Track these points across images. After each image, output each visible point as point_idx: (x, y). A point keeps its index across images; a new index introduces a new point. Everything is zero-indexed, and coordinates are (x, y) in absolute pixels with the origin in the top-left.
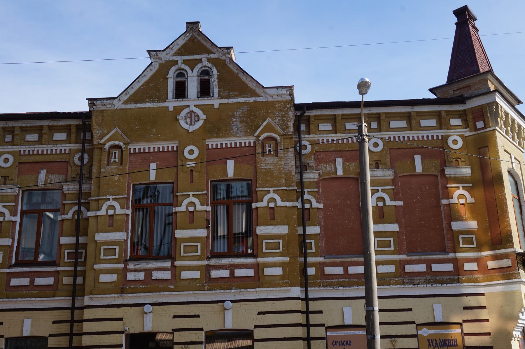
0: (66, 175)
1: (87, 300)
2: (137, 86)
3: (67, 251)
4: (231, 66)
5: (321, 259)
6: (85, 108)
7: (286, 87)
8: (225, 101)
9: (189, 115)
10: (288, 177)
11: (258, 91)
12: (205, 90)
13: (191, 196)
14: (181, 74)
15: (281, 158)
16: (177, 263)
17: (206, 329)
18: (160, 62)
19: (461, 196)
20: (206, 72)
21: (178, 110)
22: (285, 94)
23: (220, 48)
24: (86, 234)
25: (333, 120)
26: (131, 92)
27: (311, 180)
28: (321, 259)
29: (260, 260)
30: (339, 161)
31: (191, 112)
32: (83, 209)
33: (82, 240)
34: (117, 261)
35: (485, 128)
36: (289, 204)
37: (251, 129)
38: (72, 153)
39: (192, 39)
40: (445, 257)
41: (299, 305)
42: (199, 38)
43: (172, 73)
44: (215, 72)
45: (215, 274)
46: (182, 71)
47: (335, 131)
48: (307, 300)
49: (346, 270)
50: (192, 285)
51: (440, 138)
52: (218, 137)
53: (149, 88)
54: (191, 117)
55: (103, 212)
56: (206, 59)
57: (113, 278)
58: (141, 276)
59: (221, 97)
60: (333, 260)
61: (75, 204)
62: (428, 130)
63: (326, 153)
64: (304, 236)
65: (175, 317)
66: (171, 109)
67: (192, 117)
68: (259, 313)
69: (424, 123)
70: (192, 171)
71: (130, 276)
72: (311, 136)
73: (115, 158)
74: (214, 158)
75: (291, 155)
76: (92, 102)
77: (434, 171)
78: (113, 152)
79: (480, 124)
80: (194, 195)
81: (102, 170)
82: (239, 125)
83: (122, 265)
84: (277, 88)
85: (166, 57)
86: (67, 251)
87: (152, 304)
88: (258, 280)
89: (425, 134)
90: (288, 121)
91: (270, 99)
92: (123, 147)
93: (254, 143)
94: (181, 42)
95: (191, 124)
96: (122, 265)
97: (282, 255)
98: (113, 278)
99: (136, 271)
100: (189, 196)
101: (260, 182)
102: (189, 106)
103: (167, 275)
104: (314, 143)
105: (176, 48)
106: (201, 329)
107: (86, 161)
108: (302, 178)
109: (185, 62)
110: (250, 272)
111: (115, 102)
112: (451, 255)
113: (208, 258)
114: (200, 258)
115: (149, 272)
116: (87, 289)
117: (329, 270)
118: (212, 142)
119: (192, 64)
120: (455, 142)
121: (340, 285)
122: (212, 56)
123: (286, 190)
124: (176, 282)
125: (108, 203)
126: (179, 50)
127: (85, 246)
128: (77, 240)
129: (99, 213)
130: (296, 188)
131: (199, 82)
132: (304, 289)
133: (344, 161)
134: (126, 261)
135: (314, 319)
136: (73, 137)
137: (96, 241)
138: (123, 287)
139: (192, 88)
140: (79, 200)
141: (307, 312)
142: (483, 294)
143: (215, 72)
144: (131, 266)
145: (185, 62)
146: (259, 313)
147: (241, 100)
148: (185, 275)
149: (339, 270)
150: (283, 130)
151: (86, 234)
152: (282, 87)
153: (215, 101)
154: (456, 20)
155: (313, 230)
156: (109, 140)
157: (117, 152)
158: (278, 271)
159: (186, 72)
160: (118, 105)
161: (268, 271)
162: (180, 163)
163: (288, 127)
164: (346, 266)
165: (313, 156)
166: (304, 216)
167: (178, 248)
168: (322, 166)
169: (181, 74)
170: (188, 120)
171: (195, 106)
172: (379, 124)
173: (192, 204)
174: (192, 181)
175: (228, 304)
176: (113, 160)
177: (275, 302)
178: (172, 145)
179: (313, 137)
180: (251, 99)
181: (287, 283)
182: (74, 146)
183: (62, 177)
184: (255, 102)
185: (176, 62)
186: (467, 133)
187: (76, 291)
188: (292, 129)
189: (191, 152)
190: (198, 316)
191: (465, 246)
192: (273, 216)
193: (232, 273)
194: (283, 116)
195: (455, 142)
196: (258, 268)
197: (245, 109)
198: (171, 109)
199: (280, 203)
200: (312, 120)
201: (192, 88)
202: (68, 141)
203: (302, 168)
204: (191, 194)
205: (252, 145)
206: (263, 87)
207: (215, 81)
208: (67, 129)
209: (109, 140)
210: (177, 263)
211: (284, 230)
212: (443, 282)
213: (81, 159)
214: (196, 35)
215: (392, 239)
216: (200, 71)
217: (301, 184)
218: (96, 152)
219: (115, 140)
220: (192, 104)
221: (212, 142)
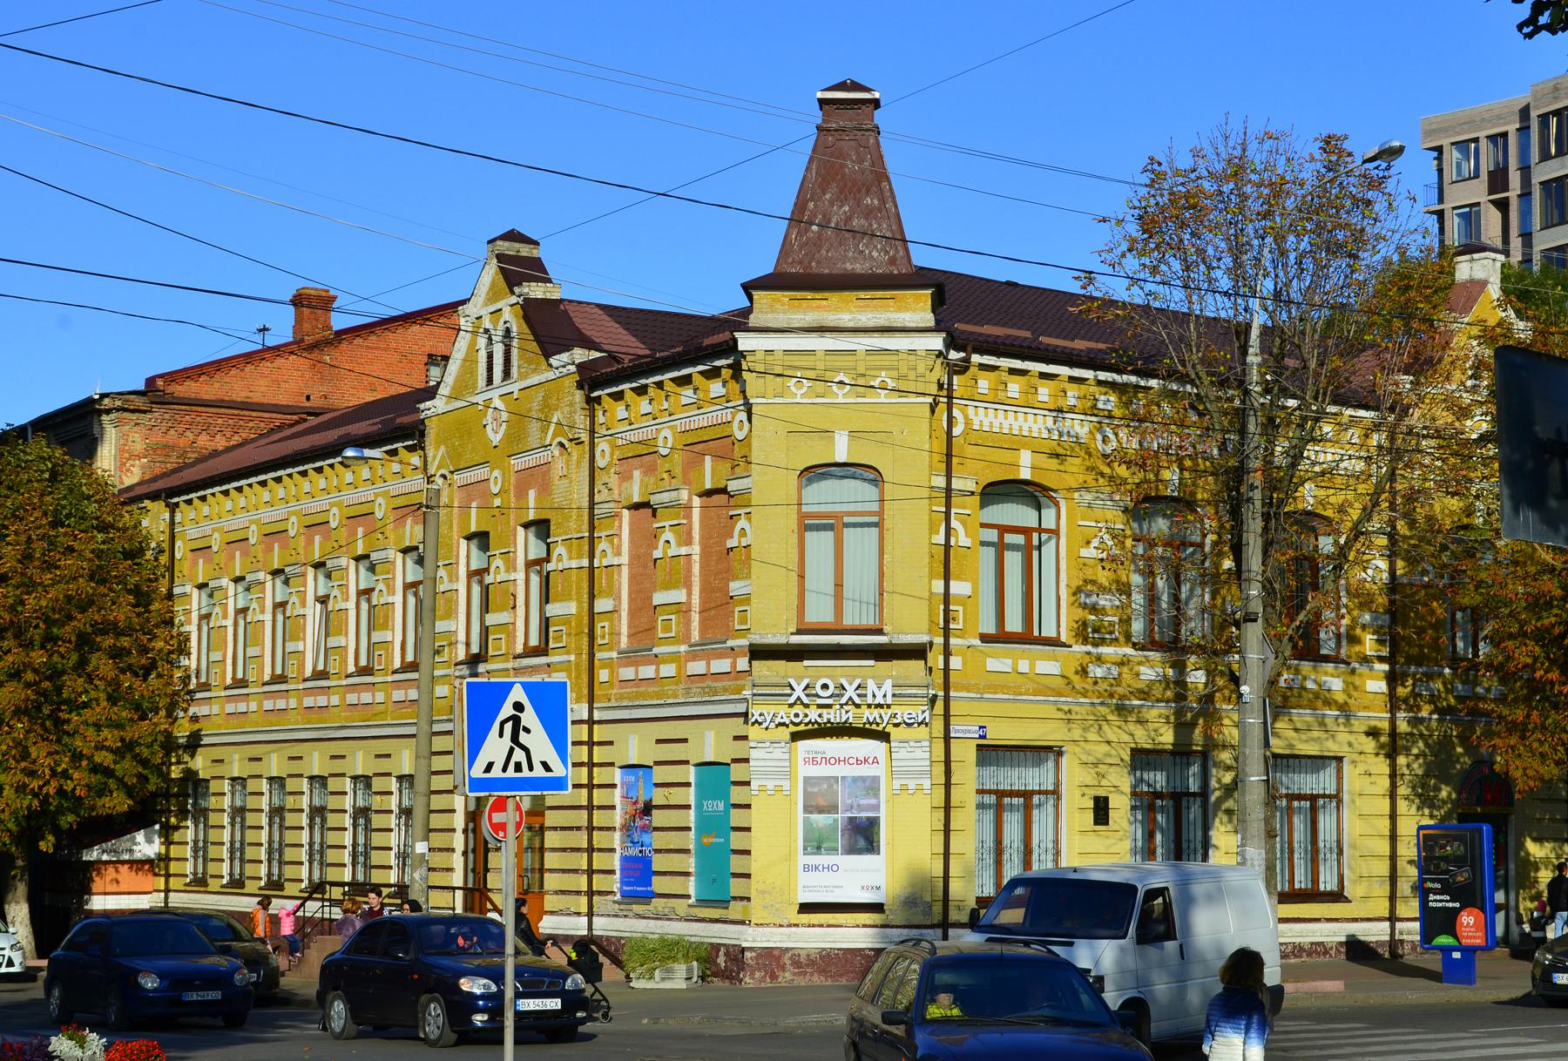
20: (508, 331)
30: (637, 474)
43: (482, 342)
104: (614, 447)
118: (517, 463)
135: (599, 754)
153: (515, 388)
155: (602, 605)
194: (571, 405)
195: (741, 429)
199: (566, 564)
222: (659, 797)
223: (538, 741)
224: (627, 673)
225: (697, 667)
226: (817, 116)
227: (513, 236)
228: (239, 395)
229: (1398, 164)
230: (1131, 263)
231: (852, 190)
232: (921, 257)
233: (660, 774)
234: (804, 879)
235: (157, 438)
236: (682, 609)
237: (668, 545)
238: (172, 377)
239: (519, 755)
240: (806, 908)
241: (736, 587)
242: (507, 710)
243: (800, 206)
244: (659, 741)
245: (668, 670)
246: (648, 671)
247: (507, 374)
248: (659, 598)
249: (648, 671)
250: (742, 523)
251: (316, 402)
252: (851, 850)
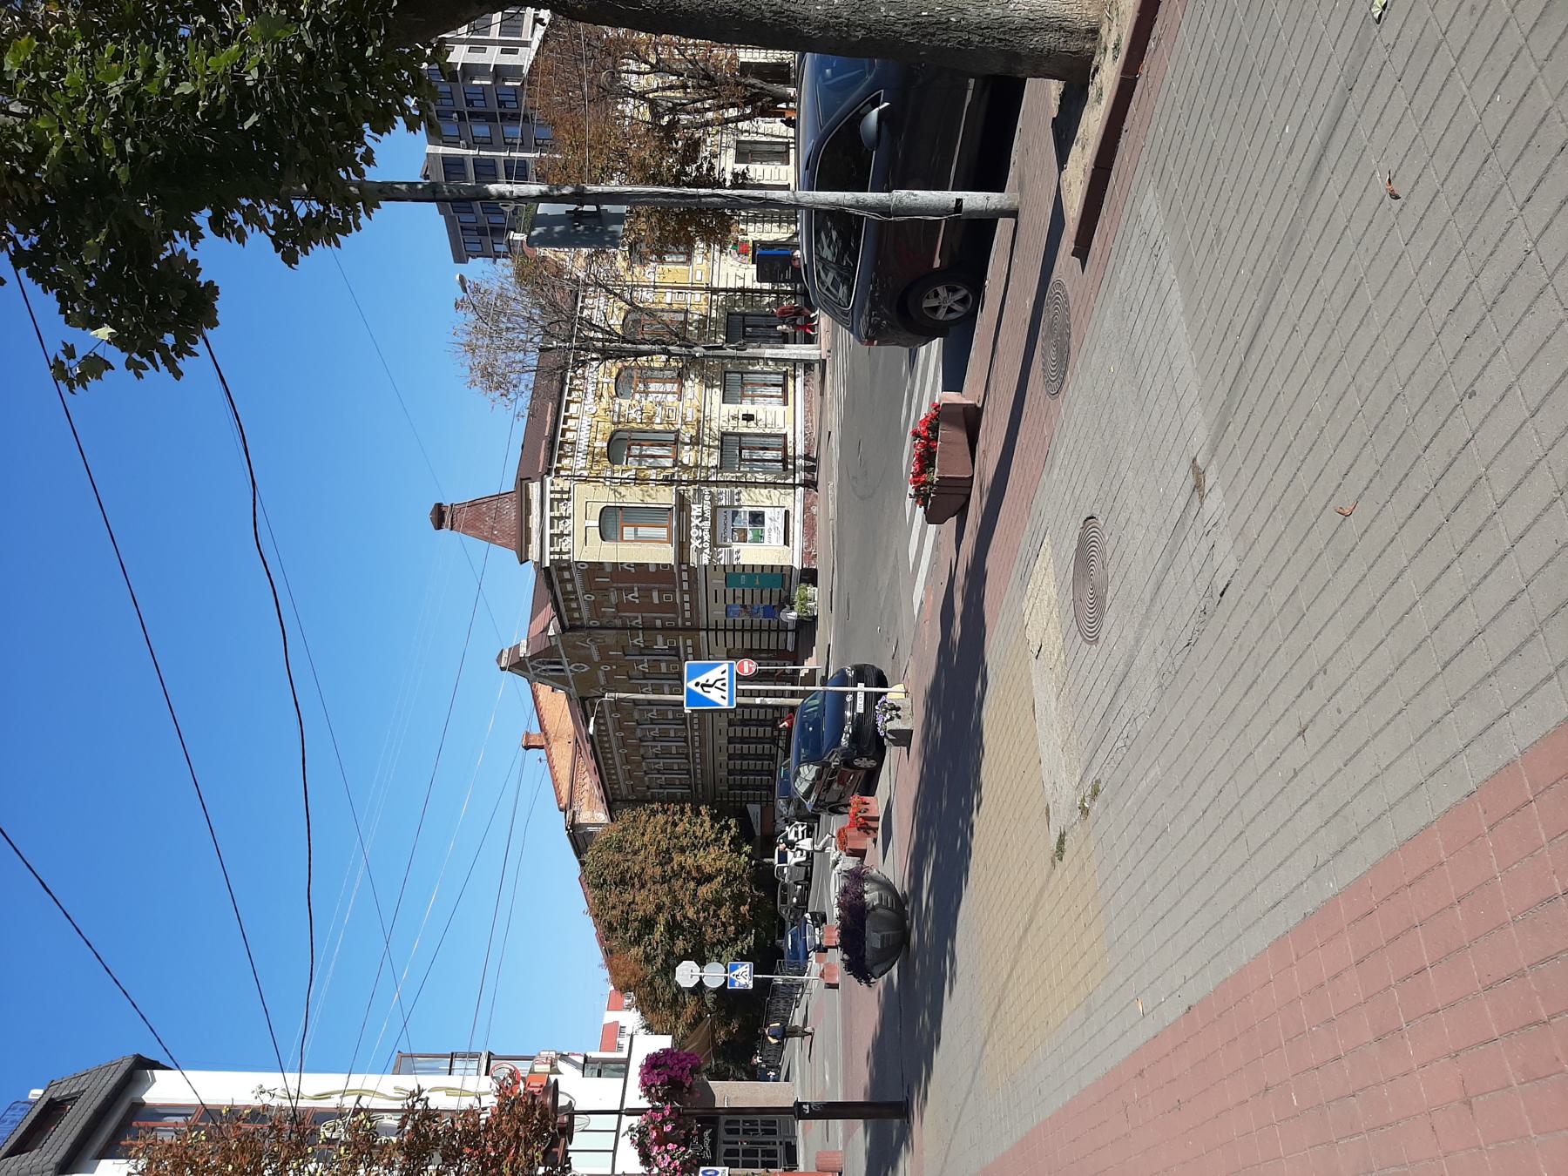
41: (711, 634)
74: (605, 659)
118: (596, 659)
141: (716, 630)
153: (565, 660)
155: (659, 623)
158: (689, 642)
166: (648, 628)
178: (601, 674)
211: (660, 639)
222: (739, 602)
223: (712, 676)
224: (687, 614)
225: (685, 586)
226: (445, 531)
227: (499, 660)
228: (567, 772)
229: (467, 278)
230: (512, 396)
231: (479, 517)
232: (509, 486)
233: (730, 601)
234: (774, 542)
235: (585, 807)
236: (660, 591)
238: (559, 801)
239: (718, 684)
240: (786, 543)
241: (652, 569)
242: (699, 690)
243: (486, 539)
245: (686, 597)
246: (687, 606)
247: (559, 663)
248: (656, 601)
249: (687, 606)
251: (572, 739)
252: (763, 523)
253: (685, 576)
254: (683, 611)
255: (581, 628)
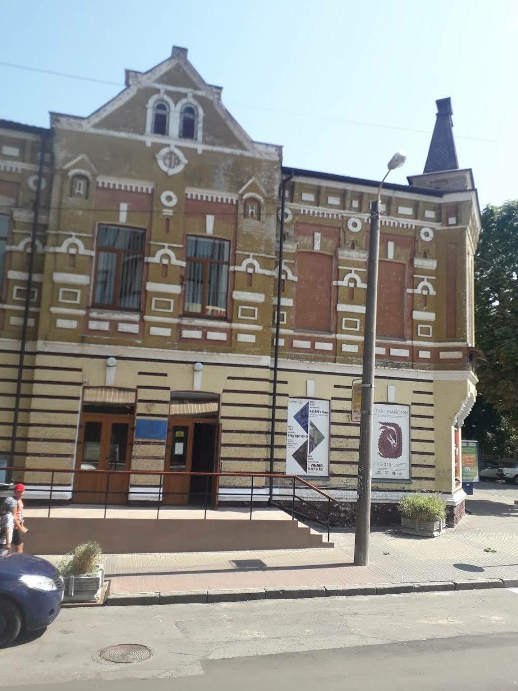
0: (17, 198)
1: (40, 345)
2: (110, 109)
3: (16, 288)
4: (219, 110)
5: (291, 332)
6: (45, 124)
7: (276, 146)
8: (210, 148)
9: (169, 156)
10: (268, 243)
11: (245, 144)
12: (188, 131)
13: (166, 247)
14: (161, 106)
15: (263, 222)
16: (147, 318)
17: (172, 389)
18: (140, 86)
19: (425, 288)
20: (190, 110)
21: (159, 147)
22: (272, 153)
23: (210, 86)
24: (41, 271)
25: (317, 191)
26: (104, 114)
27: (290, 251)
28: (291, 332)
29: (235, 325)
30: (318, 235)
31: (171, 153)
32: (37, 242)
33: (36, 278)
34: (78, 307)
35: (457, 224)
36: (268, 273)
37: (236, 185)
38: (25, 174)
39: (178, 68)
40: (403, 343)
42: (186, 68)
43: (152, 102)
44: (201, 112)
45: (186, 334)
46: (164, 103)
47: (317, 203)
48: (275, 369)
49: (313, 345)
50: (161, 342)
51: (414, 227)
52: (199, 187)
53: (125, 114)
54: (170, 159)
55: (63, 249)
56: (192, 95)
57: (73, 324)
58: (105, 326)
59: (205, 142)
60: (301, 334)
61: (28, 235)
62: (404, 218)
63: (307, 225)
64: (278, 307)
65: (140, 373)
66: (149, 144)
67: (172, 159)
68: (229, 378)
69: (402, 210)
70: (168, 220)
71: (93, 325)
72: (294, 204)
73: (79, 189)
74: (194, 210)
75: (272, 221)
76: (55, 117)
77: (404, 260)
78: (78, 183)
79: (452, 220)
80: (169, 247)
81: (64, 201)
82: (222, 179)
83: (82, 312)
84: (267, 145)
85: (146, 82)
86: (16, 288)
87: (118, 358)
88: (230, 345)
89: (403, 221)
90: (274, 183)
91: (258, 156)
92: (91, 178)
93: (237, 201)
94: (165, 69)
95: (170, 166)
96: (82, 312)
97: (255, 323)
98: (73, 324)
99: (98, 320)
100: (164, 247)
101: (239, 245)
102: (169, 145)
103: (134, 329)
105: (159, 73)
106: (168, 389)
107: (43, 186)
108: (281, 248)
109: (168, 93)
110: (223, 337)
111: (84, 123)
112: (409, 342)
113: (180, 317)
114: (171, 315)
115: (114, 324)
116: (41, 332)
117: (297, 344)
118: (193, 192)
119: (177, 97)
120: (427, 234)
121: (306, 359)
122: (199, 93)
123: (265, 257)
124: (144, 338)
125: (70, 240)
126: (162, 76)
127: (39, 285)
128: (30, 277)
129: (58, 250)
130: (276, 257)
131: (183, 118)
132: (274, 359)
133: (322, 236)
134: (88, 308)
135: (280, 388)
136: (28, 155)
137: (53, 282)
138: (83, 336)
139: (174, 125)
140: (34, 232)
141: (275, 382)
142: (431, 381)
143: (201, 112)
144: (94, 314)
145: (168, 93)
146: (229, 378)
147: (228, 150)
148: (155, 331)
149: (306, 345)
150: (268, 192)
151: (41, 271)
152: (273, 146)
154: (436, 111)
155: (287, 302)
156: (74, 166)
157: (82, 183)
158: (251, 339)
159: (169, 105)
160: (87, 128)
161: (242, 338)
162: (155, 209)
163: (273, 190)
164: (313, 341)
165: (293, 227)
166: (280, 287)
167: (148, 302)
168: (300, 238)
169: (161, 106)
170: (167, 162)
171: (177, 147)
172: (360, 204)
173: (167, 256)
174: (168, 231)
175: (199, 366)
176: (77, 191)
177: (246, 368)
178: (147, 186)
179: (295, 206)
180: (238, 152)
181: (259, 351)
182: (27, 166)
183: (11, 201)
184: (241, 156)
185: (158, 91)
186: (438, 227)
187: (26, 334)
188: (276, 193)
189: (169, 199)
190: (165, 375)
191: (422, 335)
192: (250, 281)
193: (205, 335)
196: (231, 333)
197: (230, 162)
198: (149, 144)
199: (258, 270)
200: (297, 187)
201: (174, 125)
202: (22, 158)
203: (283, 237)
204: (166, 245)
205: (234, 202)
206: (252, 142)
207: (200, 122)
208: (21, 144)
209: (74, 166)
210: (147, 318)
211: (259, 298)
212: (399, 366)
213: (38, 183)
214: (182, 63)
215: (358, 321)
216: (183, 108)
217: (280, 254)
218: (57, 180)
219: (83, 168)
220: (173, 143)
221: (193, 192)
237: (352, 279)
241: (418, 315)
244: (335, 386)
248: (341, 307)
250: (425, 283)
253: (405, 353)
254: (313, 341)
255: (282, 198)
